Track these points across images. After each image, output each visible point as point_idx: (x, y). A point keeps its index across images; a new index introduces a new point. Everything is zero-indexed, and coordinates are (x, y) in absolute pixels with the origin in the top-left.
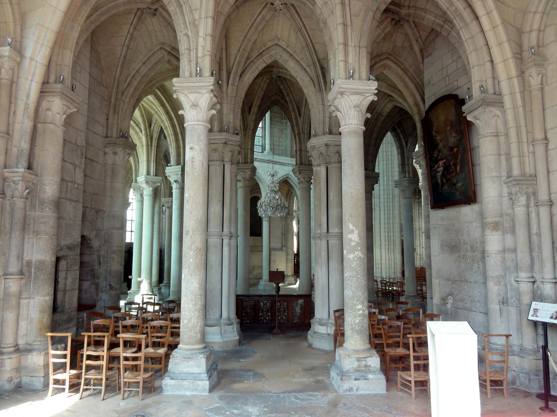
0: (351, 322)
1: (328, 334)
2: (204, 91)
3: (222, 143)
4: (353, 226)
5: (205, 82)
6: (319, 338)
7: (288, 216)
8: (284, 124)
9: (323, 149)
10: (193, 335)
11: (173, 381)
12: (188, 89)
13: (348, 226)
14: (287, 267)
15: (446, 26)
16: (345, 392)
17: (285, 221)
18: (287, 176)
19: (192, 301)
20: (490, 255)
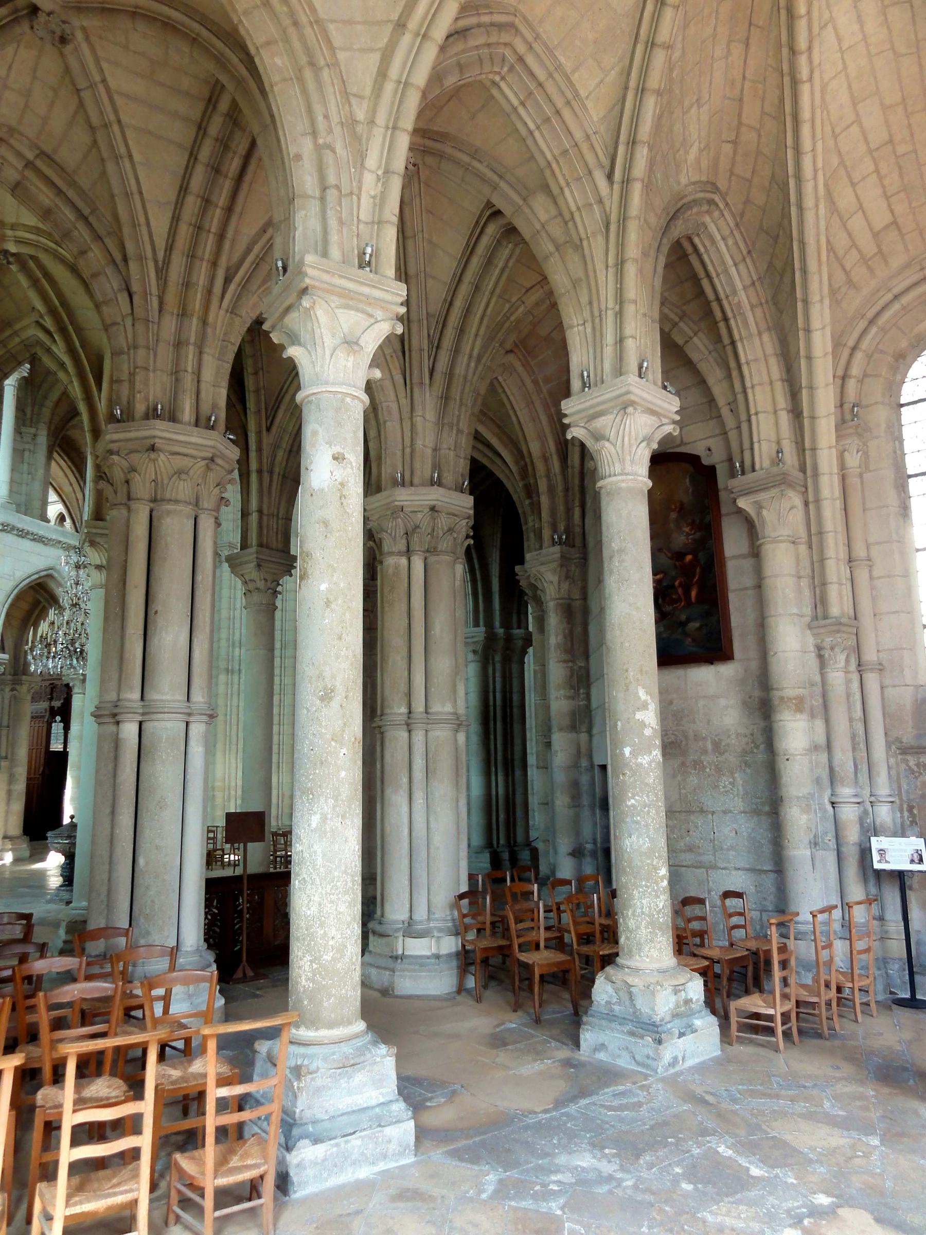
0: (650, 907)
1: (437, 957)
2: (379, 314)
3: (204, 459)
4: (647, 693)
5: (387, 291)
6: (414, 971)
7: (24, 678)
8: (28, 438)
9: (422, 519)
10: (349, 993)
11: (319, 1146)
12: (341, 296)
13: (637, 693)
14: (7, 813)
15: (681, 324)
16: (667, 1070)
17: (12, 690)
18: (50, 572)
19: (346, 893)
20: (791, 758)
